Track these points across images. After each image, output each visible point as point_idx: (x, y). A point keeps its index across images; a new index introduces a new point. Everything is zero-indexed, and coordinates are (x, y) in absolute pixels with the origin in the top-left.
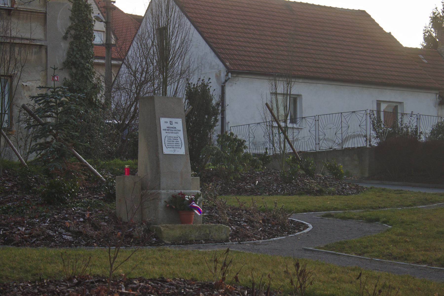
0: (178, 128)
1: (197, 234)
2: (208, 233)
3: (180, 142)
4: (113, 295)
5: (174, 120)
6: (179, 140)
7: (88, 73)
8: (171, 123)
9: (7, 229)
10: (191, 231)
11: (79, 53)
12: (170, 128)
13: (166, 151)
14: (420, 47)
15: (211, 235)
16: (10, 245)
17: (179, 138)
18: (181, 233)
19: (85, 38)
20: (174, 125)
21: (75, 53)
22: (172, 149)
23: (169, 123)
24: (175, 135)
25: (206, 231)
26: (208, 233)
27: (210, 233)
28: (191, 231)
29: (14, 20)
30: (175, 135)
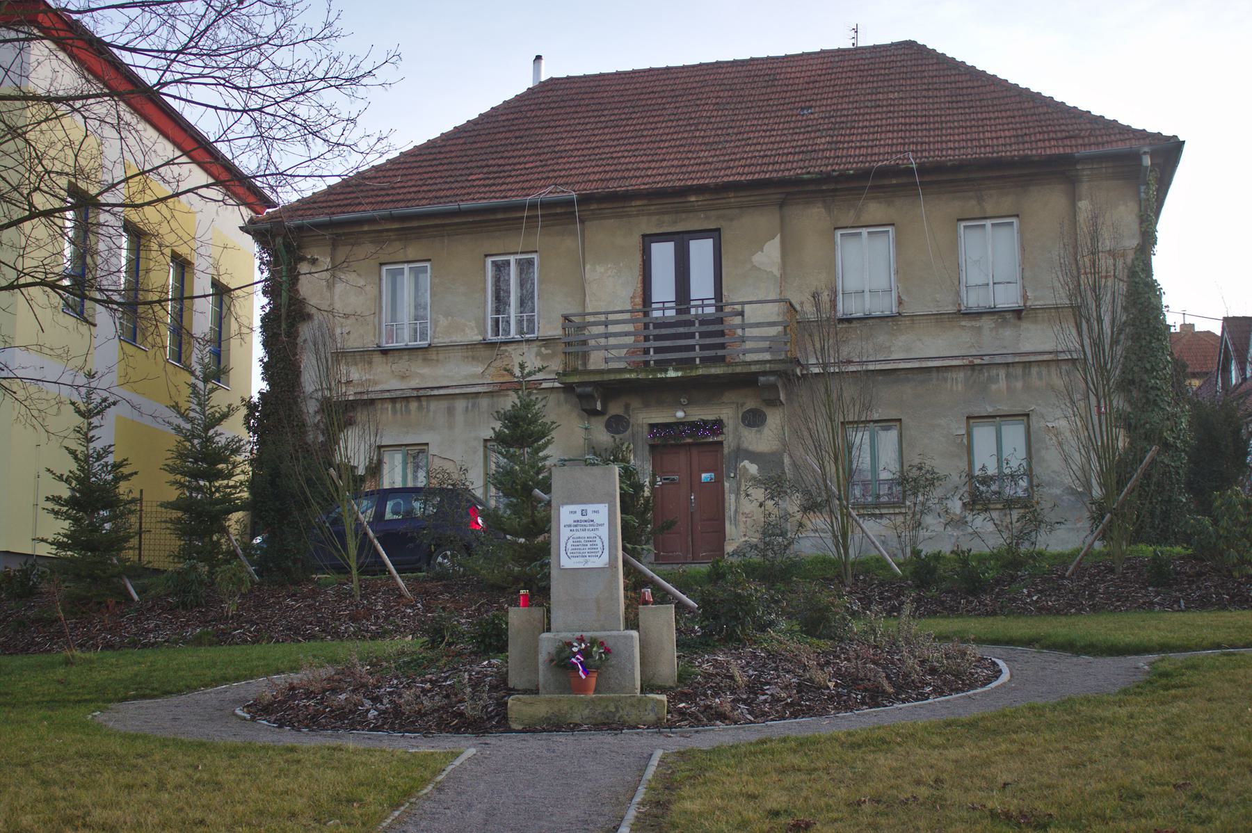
0: (597, 521)
1: (586, 712)
2: (614, 710)
3: (600, 545)
4: (1046, 831)
5: (590, 508)
6: (598, 541)
7: (1157, 395)
8: (584, 513)
9: (822, 687)
10: (571, 708)
11: (1139, 363)
12: (581, 521)
13: (566, 562)
14: (1174, 320)
15: (618, 715)
16: (341, 727)
17: (598, 538)
18: (551, 711)
19: (1148, 338)
20: (590, 516)
21: (1132, 364)
22: (582, 559)
23: (579, 513)
24: (591, 534)
25: (607, 706)
26: (614, 710)
27: (617, 711)
28: (571, 708)
29: (1025, 325)
30: (591, 534)
